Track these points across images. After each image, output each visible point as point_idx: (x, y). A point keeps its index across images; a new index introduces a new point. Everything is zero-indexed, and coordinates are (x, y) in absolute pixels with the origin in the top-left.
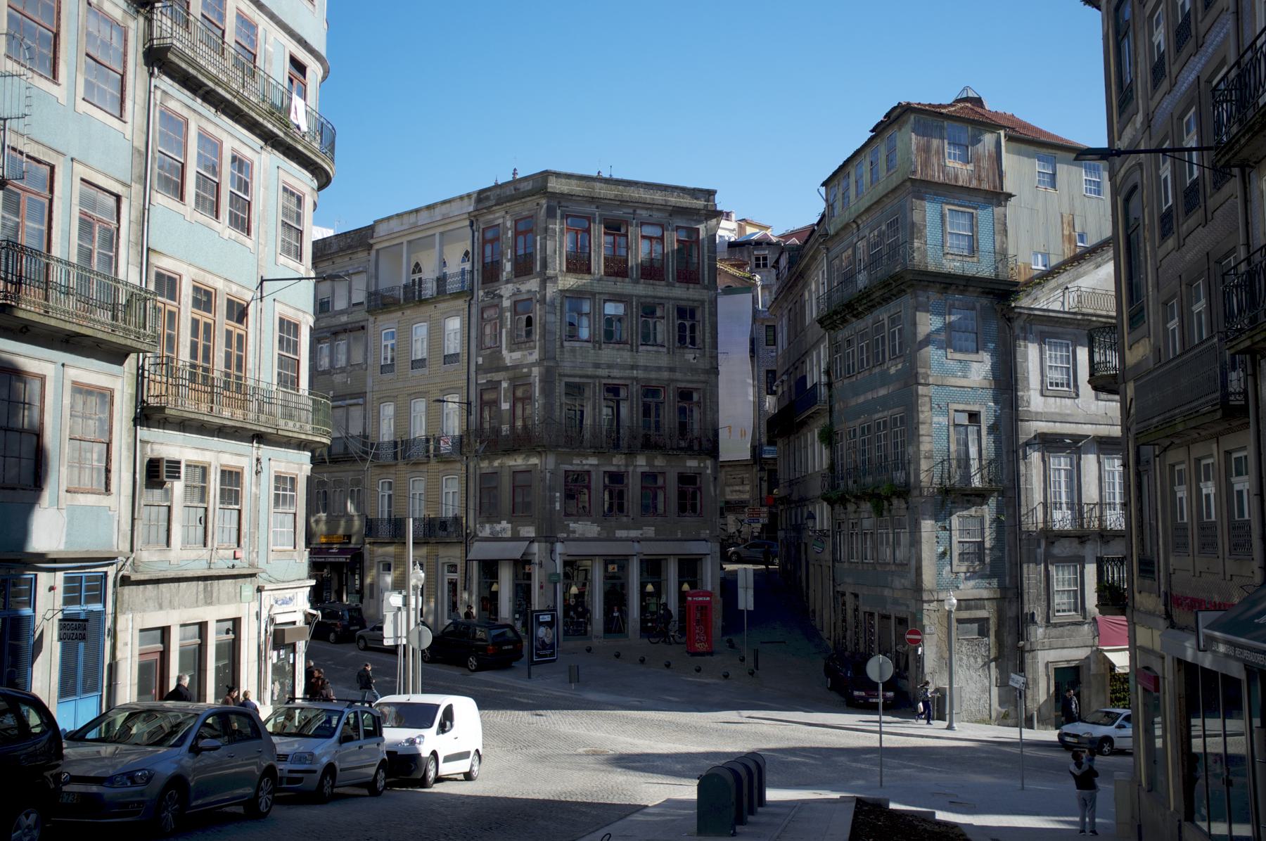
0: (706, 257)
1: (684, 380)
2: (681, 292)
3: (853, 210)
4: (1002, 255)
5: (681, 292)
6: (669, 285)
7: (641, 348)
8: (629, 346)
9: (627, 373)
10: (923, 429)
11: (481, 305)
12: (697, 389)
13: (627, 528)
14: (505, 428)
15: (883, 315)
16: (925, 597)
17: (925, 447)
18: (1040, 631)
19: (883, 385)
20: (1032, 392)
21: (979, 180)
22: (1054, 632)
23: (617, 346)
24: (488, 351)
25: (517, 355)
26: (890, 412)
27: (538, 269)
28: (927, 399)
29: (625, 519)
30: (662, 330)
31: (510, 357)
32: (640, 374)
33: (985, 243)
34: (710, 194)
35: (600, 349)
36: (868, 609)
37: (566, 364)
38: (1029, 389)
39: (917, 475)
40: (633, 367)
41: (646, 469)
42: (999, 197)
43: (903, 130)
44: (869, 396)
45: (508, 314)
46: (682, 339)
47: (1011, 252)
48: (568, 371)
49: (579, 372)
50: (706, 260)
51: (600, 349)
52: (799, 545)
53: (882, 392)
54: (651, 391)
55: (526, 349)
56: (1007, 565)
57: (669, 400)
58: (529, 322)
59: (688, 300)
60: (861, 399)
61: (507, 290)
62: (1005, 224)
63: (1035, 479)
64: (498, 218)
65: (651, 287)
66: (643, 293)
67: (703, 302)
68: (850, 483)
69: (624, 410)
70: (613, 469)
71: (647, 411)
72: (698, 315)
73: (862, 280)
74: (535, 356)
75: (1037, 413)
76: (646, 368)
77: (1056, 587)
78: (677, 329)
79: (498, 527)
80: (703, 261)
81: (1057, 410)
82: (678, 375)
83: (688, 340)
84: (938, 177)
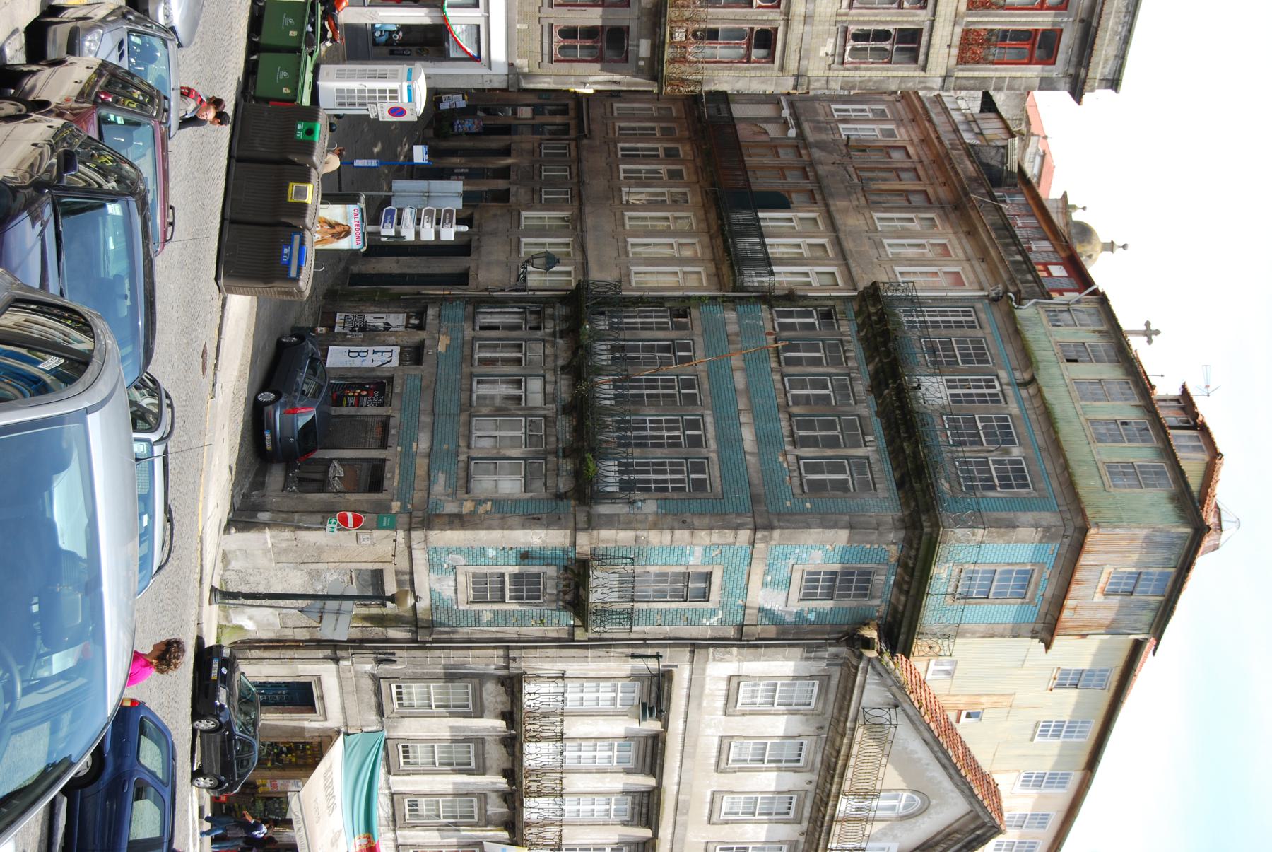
0: (1003, 74)
1: (792, 39)
3: (1054, 371)
10: (682, 535)
12: (771, 58)
15: (871, 448)
16: (417, 535)
18: (369, 667)
19: (760, 439)
20: (736, 664)
21: (1075, 609)
22: (368, 684)
26: (713, 456)
28: (731, 539)
34: (1114, 83)
38: (739, 661)
39: (611, 522)
43: (1180, 412)
44: (742, 404)
50: (998, 74)
53: (748, 435)
60: (740, 380)
63: (602, 665)
67: (924, 69)
75: (704, 670)
78: (881, 27)
80: (996, 70)
81: (707, 691)
82: (797, 28)
83: (860, 45)
84: (1085, 559)
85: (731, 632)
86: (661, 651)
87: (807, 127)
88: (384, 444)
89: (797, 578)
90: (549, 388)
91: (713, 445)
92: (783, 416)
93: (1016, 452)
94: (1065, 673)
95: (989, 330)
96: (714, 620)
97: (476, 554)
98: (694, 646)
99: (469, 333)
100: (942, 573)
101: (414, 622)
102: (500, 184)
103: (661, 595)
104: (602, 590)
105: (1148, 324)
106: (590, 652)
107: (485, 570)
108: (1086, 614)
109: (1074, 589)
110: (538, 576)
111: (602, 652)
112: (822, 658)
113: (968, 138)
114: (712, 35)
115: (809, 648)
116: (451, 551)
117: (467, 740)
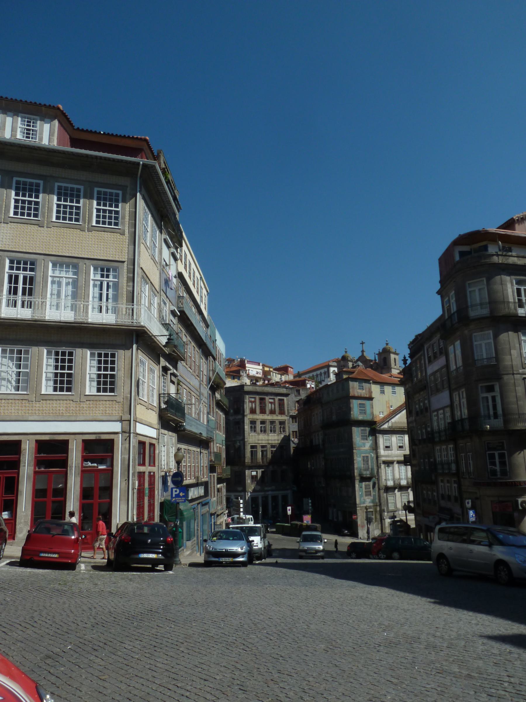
9: (267, 442)
10: (355, 462)
17: (356, 466)
18: (386, 514)
21: (366, 394)
32: (270, 442)
33: (368, 411)
40: (268, 440)
42: (371, 399)
47: (374, 413)
48: (251, 442)
49: (254, 442)
62: (373, 406)
63: (383, 473)
73: (334, 418)
76: (271, 440)
77: (389, 501)
84: (356, 395)
85: (375, 451)
86: (379, 462)
89: (363, 441)
94: (381, 393)
97: (361, 496)
98: (377, 457)
100: (361, 418)
103: (368, 464)
104: (367, 474)
106: (380, 475)
108: (367, 393)
109: (363, 396)
110: (365, 485)
112: (379, 436)
116: (360, 500)
117: (401, 496)
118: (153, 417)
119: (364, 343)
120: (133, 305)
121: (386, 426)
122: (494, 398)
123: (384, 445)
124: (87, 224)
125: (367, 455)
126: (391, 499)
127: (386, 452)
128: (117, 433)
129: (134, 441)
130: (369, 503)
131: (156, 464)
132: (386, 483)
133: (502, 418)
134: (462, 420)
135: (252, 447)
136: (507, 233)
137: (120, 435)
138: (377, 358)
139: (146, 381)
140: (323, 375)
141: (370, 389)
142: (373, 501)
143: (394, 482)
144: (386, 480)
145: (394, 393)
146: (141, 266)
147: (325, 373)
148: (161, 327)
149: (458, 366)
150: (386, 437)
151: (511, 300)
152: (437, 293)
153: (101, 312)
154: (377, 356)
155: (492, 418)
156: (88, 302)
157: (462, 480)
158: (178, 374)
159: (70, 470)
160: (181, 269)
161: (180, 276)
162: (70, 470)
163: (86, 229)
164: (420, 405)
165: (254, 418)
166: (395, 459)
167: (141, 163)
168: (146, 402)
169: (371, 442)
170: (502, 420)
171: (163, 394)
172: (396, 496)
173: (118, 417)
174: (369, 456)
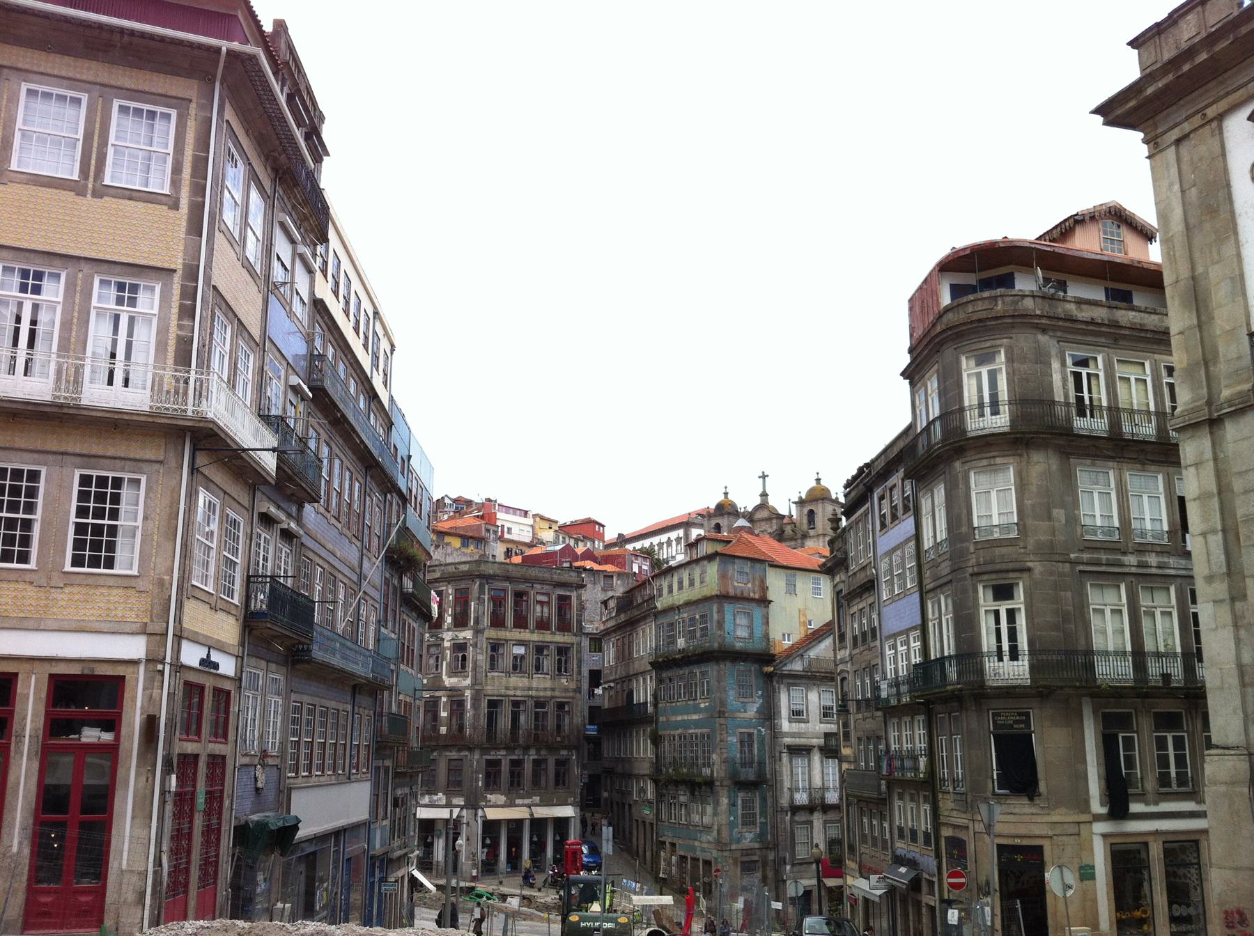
2: (560, 638)
4: (766, 636)
5: (560, 638)
6: (553, 634)
7: (534, 676)
8: (527, 675)
9: (526, 693)
11: (427, 643)
12: (568, 703)
13: (523, 798)
14: (443, 730)
15: (697, 671)
18: (788, 867)
21: (754, 593)
22: (796, 869)
23: (520, 675)
24: (432, 676)
25: (454, 680)
27: (472, 624)
29: (522, 792)
30: (548, 663)
31: (448, 681)
32: (533, 693)
33: (758, 632)
35: (509, 677)
36: (683, 854)
37: (488, 687)
40: (530, 689)
41: (536, 757)
42: (764, 602)
45: (448, 652)
46: (559, 670)
48: (489, 693)
49: (496, 693)
51: (509, 677)
52: (624, 804)
53: (695, 717)
54: (540, 703)
55: (461, 676)
56: (769, 828)
57: (551, 709)
58: (464, 658)
59: (564, 643)
60: (679, 718)
61: (448, 637)
63: (784, 773)
64: (443, 586)
65: (541, 636)
66: (536, 639)
67: (573, 644)
68: (670, 770)
69: (522, 718)
70: (515, 757)
71: (537, 719)
72: (570, 654)
73: (681, 643)
74: (468, 682)
76: (537, 689)
79: (435, 798)
81: (797, 731)
82: (557, 693)
84: (732, 592)
87: (612, 678)
88: (698, 860)
89: (741, 700)
90: (682, 793)
91: (697, 731)
92: (689, 703)
93: (697, 617)
95: (665, 620)
96: (763, 730)
99: (666, 823)
101: (766, 847)
102: (627, 807)
103: (751, 751)
105: (760, 477)
106: (778, 779)
107: (740, 821)
108: (756, 589)
109: (746, 595)
111: (778, 774)
113: (614, 614)
114: (559, 726)
115: (774, 691)
117: (825, 828)
118: (227, 629)
119: (767, 476)
120: (188, 372)
121: (797, 666)
122: (1011, 614)
123: (790, 710)
124: (91, 179)
125: (751, 730)
126: (800, 835)
127: (794, 724)
128: (134, 662)
129: (172, 683)
130: (750, 842)
131: (231, 736)
132: (792, 798)
133: (1026, 658)
134: (942, 660)
135: (493, 704)
136: (1056, 250)
137: (142, 668)
138: (794, 513)
139: (214, 546)
140: (674, 543)
141: (763, 581)
142: (761, 837)
143: (810, 795)
144: (790, 789)
145: (817, 591)
146: (213, 283)
147: (678, 540)
148: (257, 423)
149: (939, 540)
150: (797, 693)
151: (1059, 397)
152: (902, 374)
153: (110, 382)
154: (794, 507)
155: (1006, 658)
156: (83, 359)
157: (940, 796)
158: (301, 532)
159: (17, 743)
160: (324, 291)
161: (319, 306)
162: (17, 743)
163: (90, 192)
164: (861, 624)
165: (499, 637)
166: (815, 742)
167: (224, 49)
168: (212, 594)
169: (761, 701)
170: (1026, 663)
171: (262, 576)
172: (812, 828)
173: (138, 625)
174: (755, 732)
